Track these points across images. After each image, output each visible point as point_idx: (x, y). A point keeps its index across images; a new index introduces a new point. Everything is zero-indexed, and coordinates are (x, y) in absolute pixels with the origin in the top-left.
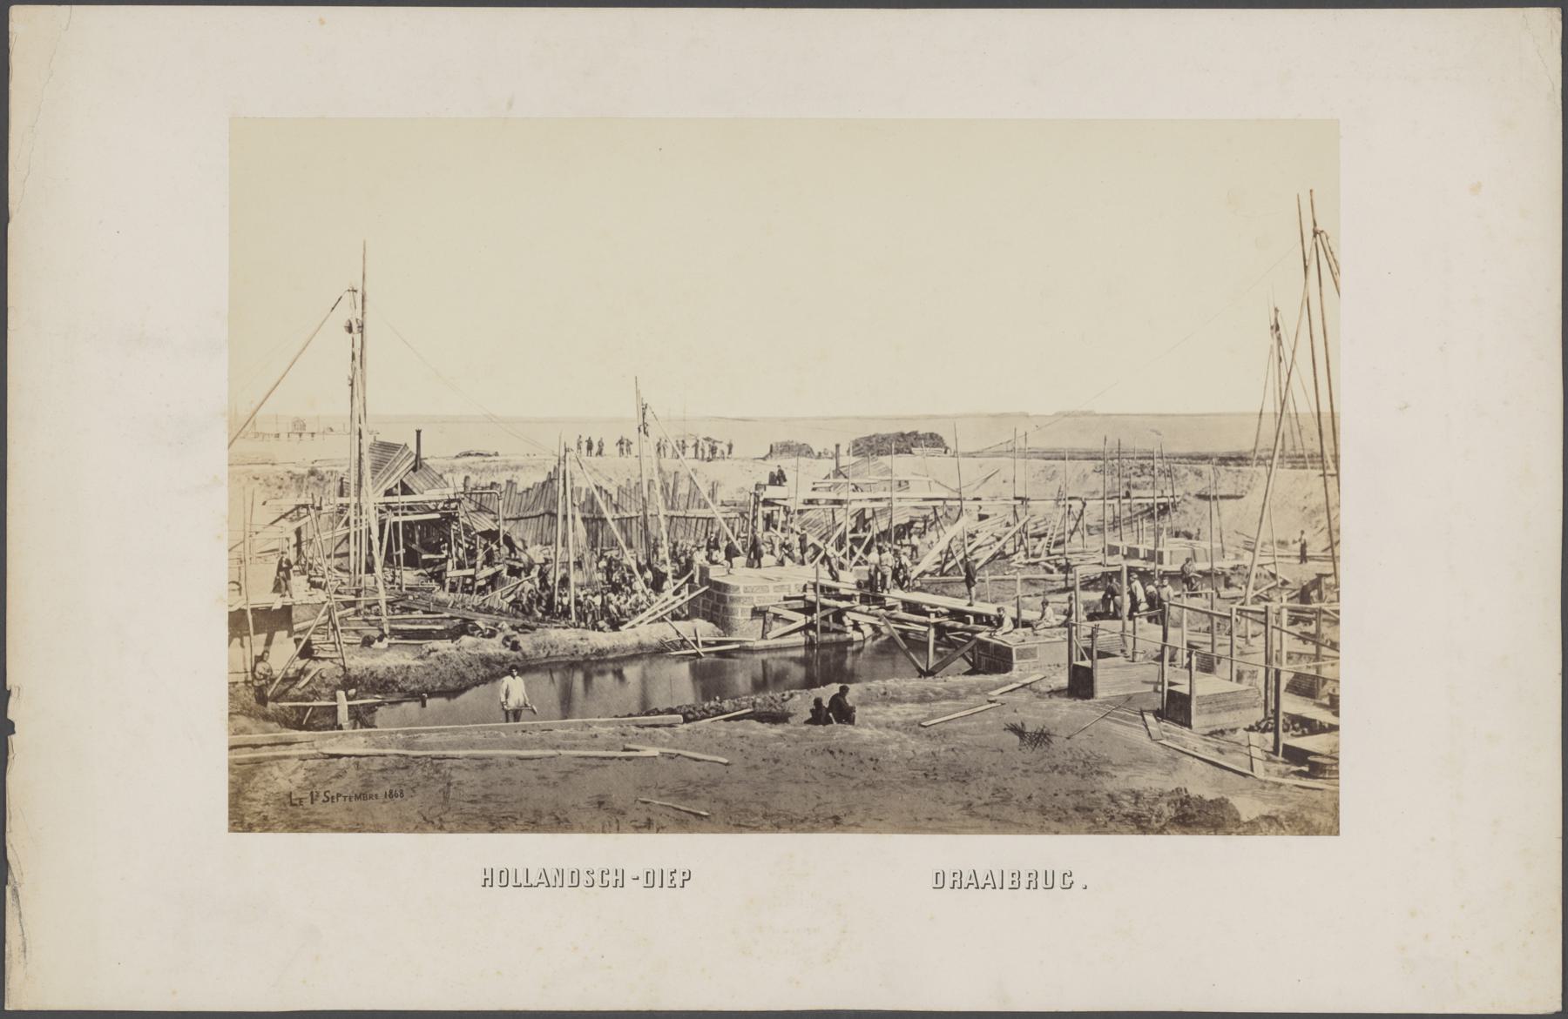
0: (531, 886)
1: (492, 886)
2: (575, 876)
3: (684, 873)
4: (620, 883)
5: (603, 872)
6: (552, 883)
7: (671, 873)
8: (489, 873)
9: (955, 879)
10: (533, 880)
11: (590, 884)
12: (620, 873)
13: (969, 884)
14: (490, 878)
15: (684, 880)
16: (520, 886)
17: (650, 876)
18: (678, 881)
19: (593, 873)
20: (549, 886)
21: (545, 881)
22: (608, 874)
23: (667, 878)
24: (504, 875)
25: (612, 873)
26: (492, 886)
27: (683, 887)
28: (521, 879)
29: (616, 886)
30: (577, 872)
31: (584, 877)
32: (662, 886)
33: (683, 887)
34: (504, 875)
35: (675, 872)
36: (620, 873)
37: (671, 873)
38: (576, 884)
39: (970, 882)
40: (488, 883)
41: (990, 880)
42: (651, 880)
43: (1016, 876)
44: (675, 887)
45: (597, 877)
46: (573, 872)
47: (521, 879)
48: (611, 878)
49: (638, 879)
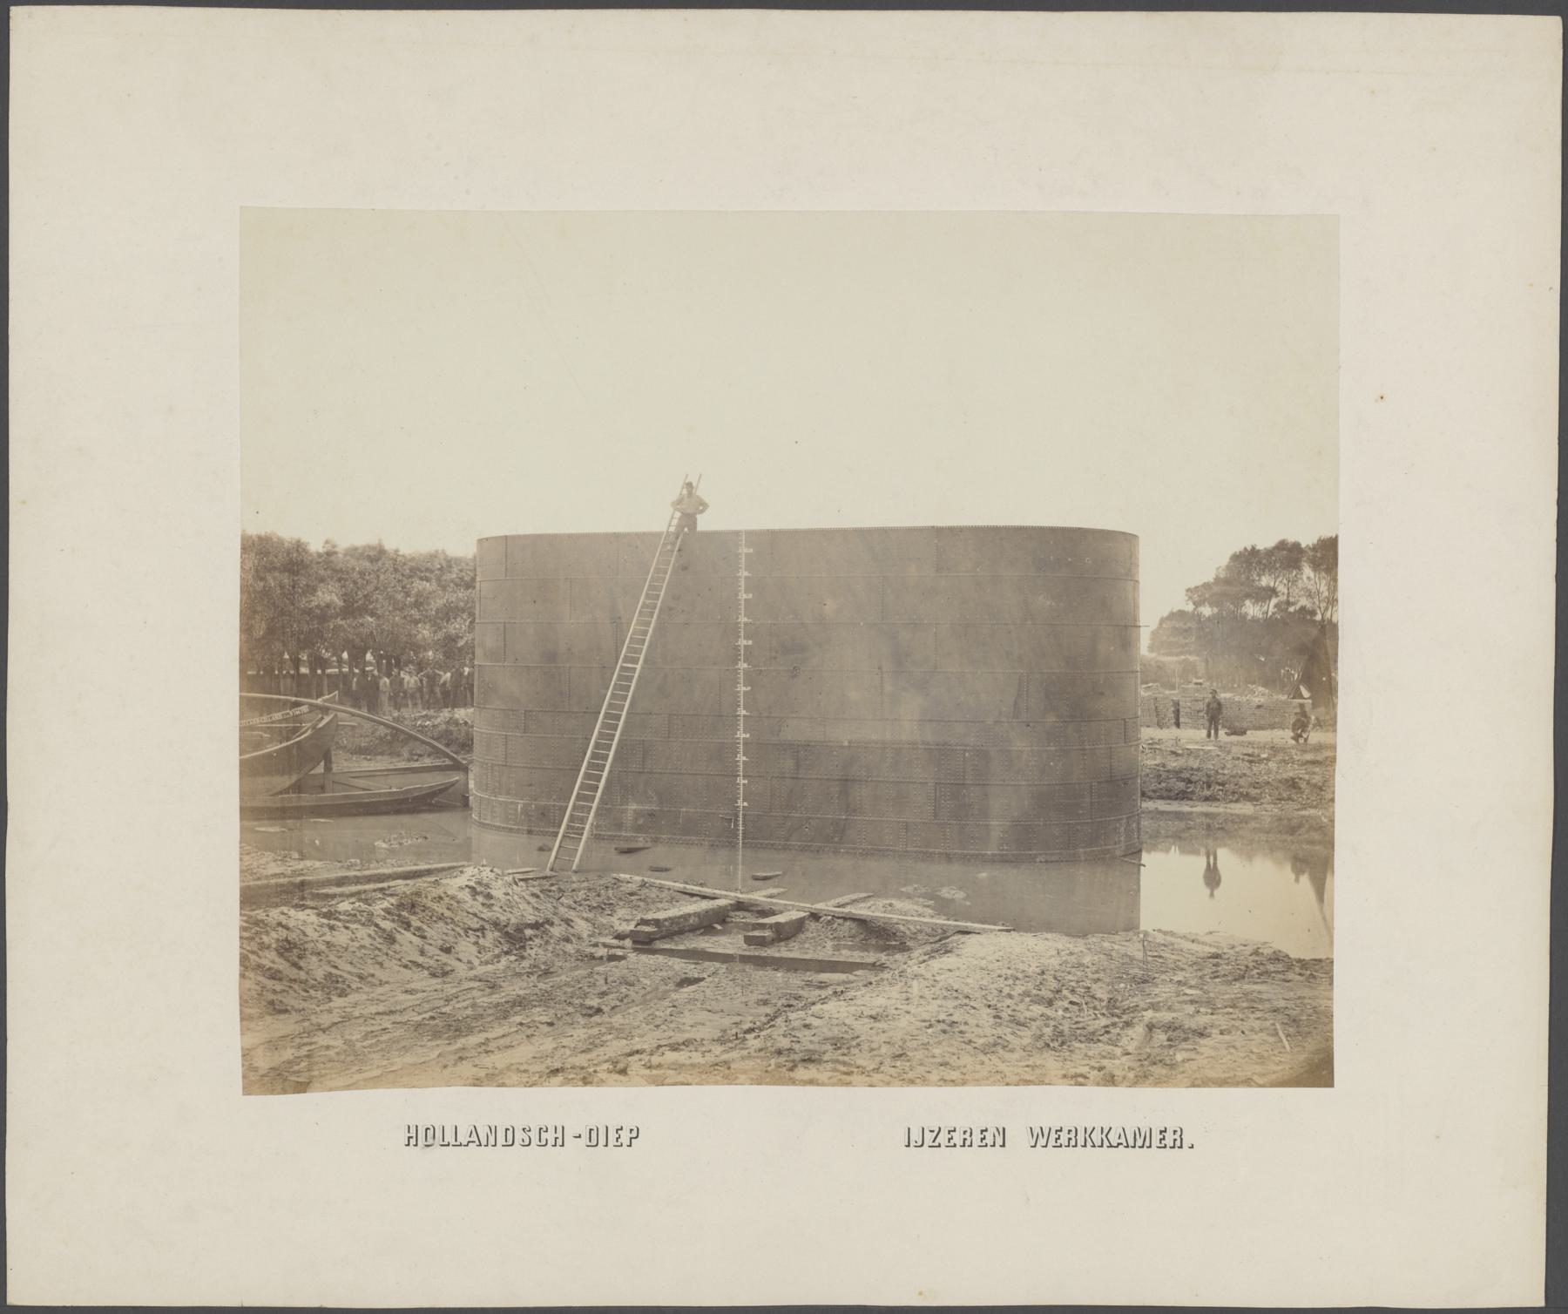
0: (461, 1145)
1: (416, 1145)
2: (510, 1133)
3: (631, 1130)
4: (559, 1142)
5: (541, 1129)
6: (484, 1142)
7: (617, 1130)
8: (413, 1130)
9: (556, 1136)
10: (463, 1138)
11: (527, 1143)
12: (559, 1130)
13: (469, 1142)
14: (414, 1135)
15: (631, 1138)
16: (448, 1145)
17: (594, 1134)
18: (625, 1139)
19: (530, 1131)
20: (480, 1145)
21: (475, 1139)
22: (547, 1131)
23: (612, 1136)
24: (430, 1133)
25: (552, 1130)
26: (416, 1145)
27: (630, 1146)
28: (449, 1138)
29: (555, 1145)
30: (511, 1129)
31: (519, 1135)
32: (606, 1146)
33: (630, 1146)
34: (430, 1133)
35: (986, 1130)
36: (559, 1130)
37: (617, 1130)
38: (510, 1143)
39: (471, 1139)
40: (413, 1141)
41: (1123, 1140)
42: (593, 1138)
43: (968, 1134)
44: (621, 1145)
45: (534, 1135)
46: (507, 1130)
47: (449, 1138)
48: (550, 1136)
49: (580, 1137)
